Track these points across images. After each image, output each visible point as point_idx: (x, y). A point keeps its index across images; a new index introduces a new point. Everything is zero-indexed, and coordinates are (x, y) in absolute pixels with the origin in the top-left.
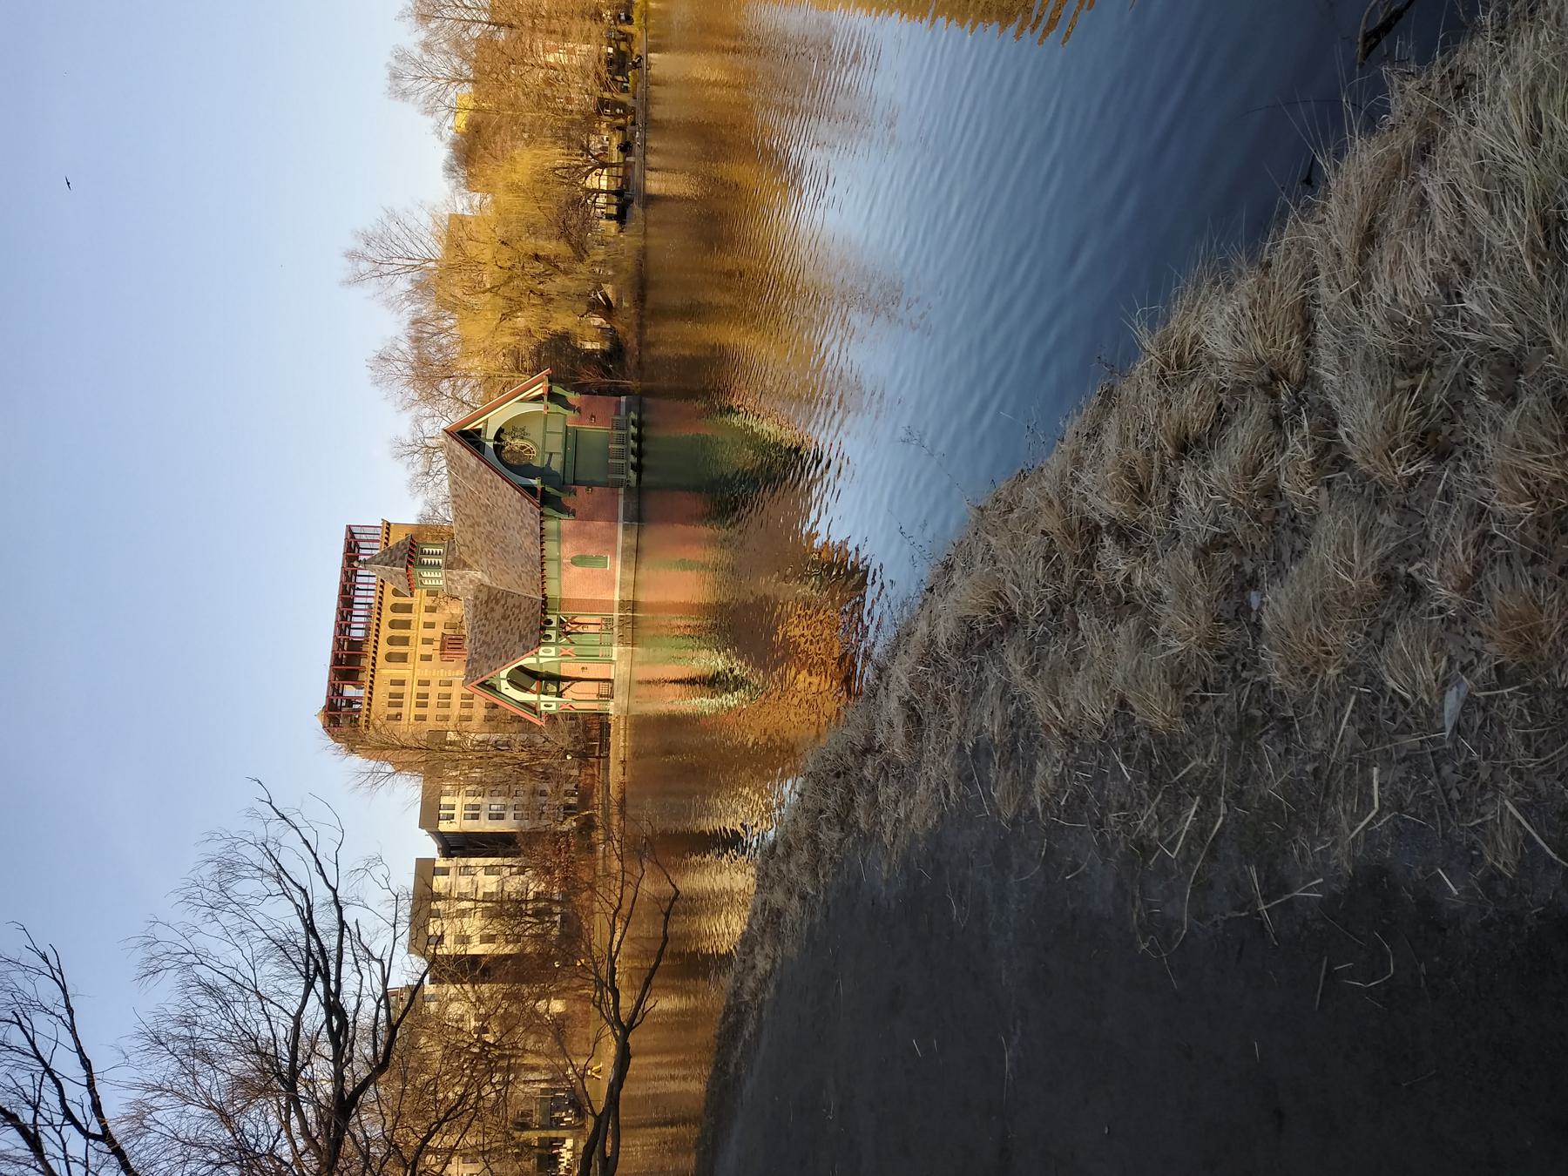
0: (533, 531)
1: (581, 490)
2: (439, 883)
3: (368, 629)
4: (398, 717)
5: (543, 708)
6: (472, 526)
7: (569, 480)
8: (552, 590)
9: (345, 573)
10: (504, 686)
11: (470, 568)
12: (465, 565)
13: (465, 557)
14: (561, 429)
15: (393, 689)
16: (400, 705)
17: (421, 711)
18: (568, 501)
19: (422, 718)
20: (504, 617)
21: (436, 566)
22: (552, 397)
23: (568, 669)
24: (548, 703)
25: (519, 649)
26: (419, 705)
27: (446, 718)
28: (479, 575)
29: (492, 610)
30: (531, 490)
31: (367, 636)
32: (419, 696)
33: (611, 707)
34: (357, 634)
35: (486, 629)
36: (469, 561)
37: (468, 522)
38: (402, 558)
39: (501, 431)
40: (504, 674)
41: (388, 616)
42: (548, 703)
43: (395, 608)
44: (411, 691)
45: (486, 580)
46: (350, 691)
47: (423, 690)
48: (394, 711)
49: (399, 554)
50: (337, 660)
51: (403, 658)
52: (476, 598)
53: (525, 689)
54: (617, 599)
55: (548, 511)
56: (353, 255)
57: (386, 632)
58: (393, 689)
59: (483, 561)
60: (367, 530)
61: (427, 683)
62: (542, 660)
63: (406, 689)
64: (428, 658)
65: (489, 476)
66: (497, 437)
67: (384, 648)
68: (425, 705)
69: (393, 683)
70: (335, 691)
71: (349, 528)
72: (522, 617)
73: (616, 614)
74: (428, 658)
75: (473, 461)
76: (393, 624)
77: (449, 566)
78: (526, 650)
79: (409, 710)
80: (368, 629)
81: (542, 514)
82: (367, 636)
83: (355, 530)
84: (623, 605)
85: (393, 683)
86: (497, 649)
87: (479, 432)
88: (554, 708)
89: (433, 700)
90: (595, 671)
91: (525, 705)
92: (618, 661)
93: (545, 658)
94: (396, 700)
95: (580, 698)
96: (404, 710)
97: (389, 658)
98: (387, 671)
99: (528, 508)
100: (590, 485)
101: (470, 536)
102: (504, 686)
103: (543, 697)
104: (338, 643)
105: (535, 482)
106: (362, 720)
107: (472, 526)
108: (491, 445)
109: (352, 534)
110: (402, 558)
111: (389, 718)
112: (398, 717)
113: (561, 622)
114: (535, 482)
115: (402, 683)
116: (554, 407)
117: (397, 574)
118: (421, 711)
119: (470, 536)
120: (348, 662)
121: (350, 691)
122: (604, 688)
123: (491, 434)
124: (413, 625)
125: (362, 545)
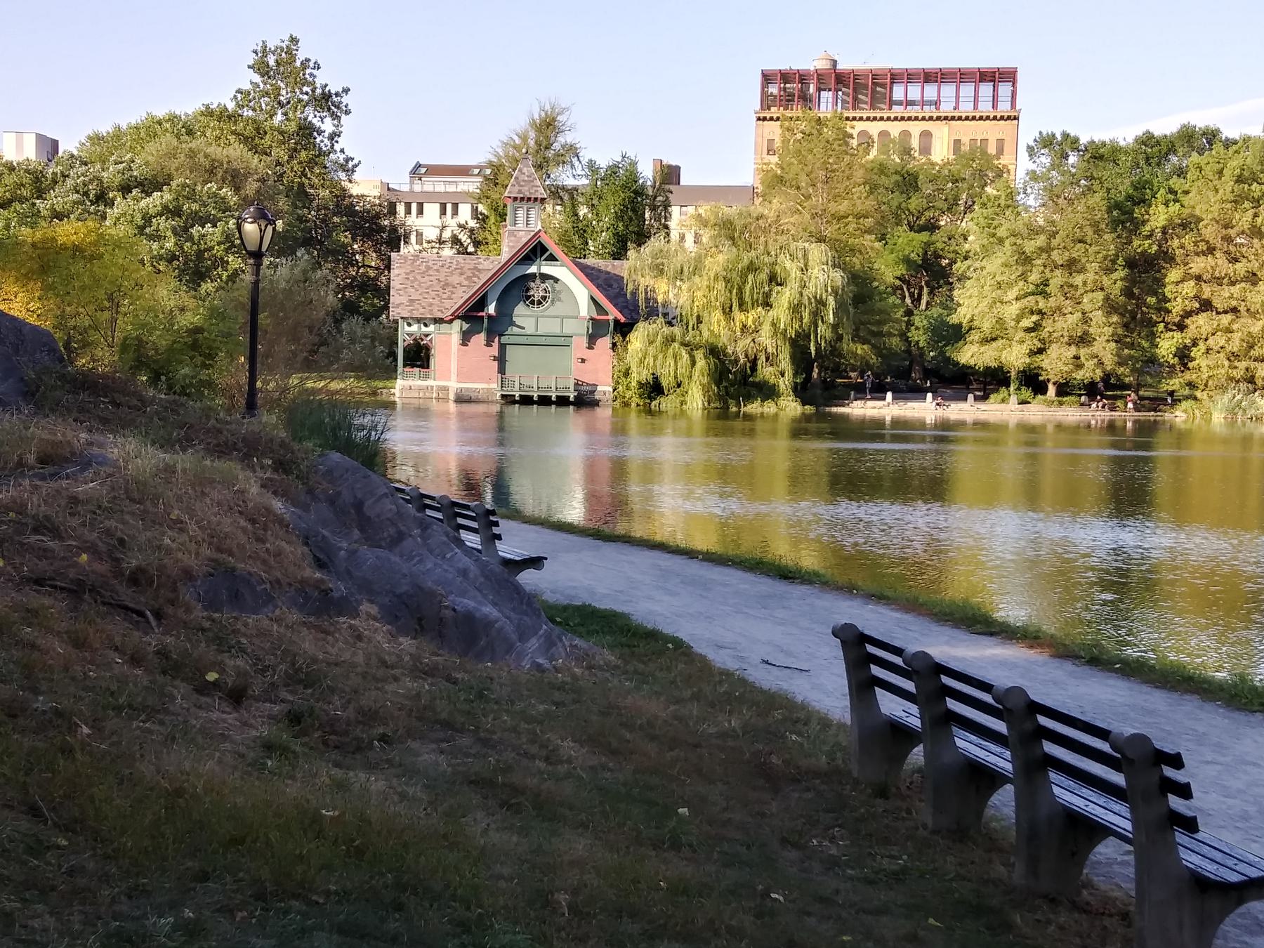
1: (494, 350)
7: (504, 340)
14: (567, 331)
31: (900, 103)
66: (545, 277)
82: (900, 103)
105: (491, 309)
108: (533, 269)
110: (520, 192)
114: (491, 309)
123: (547, 269)
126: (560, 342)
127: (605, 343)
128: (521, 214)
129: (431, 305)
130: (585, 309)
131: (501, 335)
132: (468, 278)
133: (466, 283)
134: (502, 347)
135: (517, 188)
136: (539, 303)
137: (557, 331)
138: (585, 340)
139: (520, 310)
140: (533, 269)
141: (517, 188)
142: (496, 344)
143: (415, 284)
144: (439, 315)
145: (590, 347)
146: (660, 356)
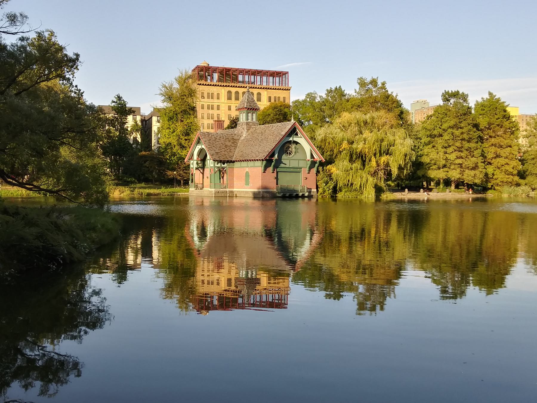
0: (257, 156)
2: (130, 118)
3: (243, 82)
4: (203, 97)
5: (191, 162)
6: (262, 133)
7: (278, 170)
8: (237, 164)
9: (267, 72)
10: (199, 147)
11: (247, 132)
12: (248, 130)
13: (251, 130)
14: (300, 166)
15: (215, 94)
16: (208, 98)
17: (206, 107)
18: (271, 168)
19: (203, 108)
20: (226, 146)
22: (313, 163)
23: (207, 171)
24: (193, 164)
25: (213, 152)
26: (208, 106)
27: (203, 118)
28: (244, 135)
29: (230, 141)
30: (273, 155)
32: (213, 106)
33: (192, 189)
34: (240, 78)
35: (222, 139)
36: (249, 131)
37: (263, 131)
38: (250, 106)
39: (296, 143)
40: (203, 147)
42: (193, 164)
44: (215, 102)
45: (242, 138)
46: (216, 76)
47: (215, 107)
48: (206, 95)
49: (252, 104)
50: (228, 70)
51: (229, 98)
52: (235, 135)
53: (199, 155)
54: (234, 190)
55: (265, 162)
56: (374, 82)
58: (215, 94)
59: (249, 137)
60: (287, 80)
61: (218, 108)
62: (208, 161)
63: (216, 100)
64: (230, 108)
65: (278, 139)
67: (233, 90)
68: (208, 108)
69: (218, 94)
70: (215, 70)
71: (288, 73)
72: (226, 153)
73: (228, 190)
74: (230, 108)
75: (283, 133)
77: (247, 124)
78: (212, 155)
79: (206, 102)
80: (243, 82)
81: (263, 160)
82: (240, 82)
83: (287, 75)
84: (232, 192)
85: (218, 94)
87: (297, 134)
88: (191, 166)
89: (211, 112)
90: (207, 182)
92: (209, 190)
93: (210, 163)
94: (211, 96)
95: (197, 175)
96: (206, 100)
97: (229, 92)
98: (223, 91)
99: (264, 155)
100: (277, 178)
101: (258, 131)
102: (199, 147)
103: (195, 162)
104: (237, 70)
105: (276, 156)
106: (203, 82)
107: (262, 133)
108: (291, 139)
110: (250, 106)
111: (203, 93)
112: (203, 97)
114: (276, 156)
115: (218, 98)
116: (309, 163)
117: (244, 104)
118: (206, 107)
119: (258, 131)
120: (228, 75)
121: (216, 76)
122: (200, 186)
123: (296, 139)
126: (297, 170)
127: (314, 170)
128: (250, 115)
129: (225, 155)
130: (309, 157)
131: (277, 168)
132: (233, 143)
133: (233, 145)
134: (277, 172)
135: (249, 104)
136: (290, 154)
137: (297, 166)
138: (307, 169)
139: (284, 156)
140: (291, 139)
141: (249, 104)
142: (275, 172)
144: (230, 159)
145: (309, 173)
146: (354, 176)
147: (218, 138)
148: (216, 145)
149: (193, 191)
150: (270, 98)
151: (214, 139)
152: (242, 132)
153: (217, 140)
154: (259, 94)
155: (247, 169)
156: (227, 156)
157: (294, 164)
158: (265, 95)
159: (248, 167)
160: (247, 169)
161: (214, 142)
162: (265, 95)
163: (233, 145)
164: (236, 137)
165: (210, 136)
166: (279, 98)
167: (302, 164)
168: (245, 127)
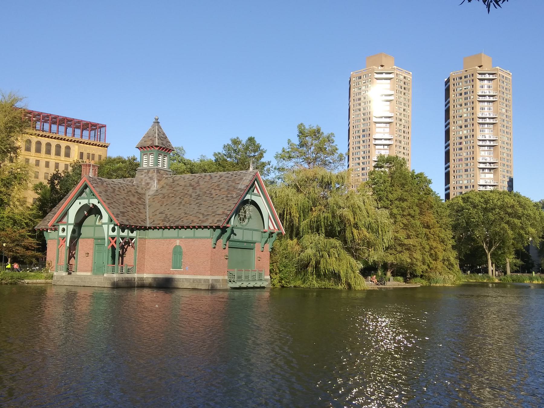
9: (79, 122)
11: (158, 183)
12: (159, 180)
14: (254, 239)
20: (131, 203)
21: (157, 163)
29: (134, 196)
35: (122, 190)
37: (193, 183)
38: (162, 144)
40: (94, 201)
41: (54, 143)
43: (58, 147)
49: (164, 142)
57: (44, 141)
59: (165, 191)
71: (104, 126)
72: (135, 214)
76: (49, 145)
83: (103, 130)
86: (112, 197)
91: (66, 213)
101: (182, 183)
109: (100, 128)
113: (132, 239)
117: (153, 141)
123: (254, 198)
124: (48, 156)
125: (93, 133)
129: (135, 217)
133: (140, 202)
143: (115, 200)
144: (142, 224)
147: (117, 189)
148: (117, 200)
149: (62, 277)
150: (82, 155)
151: (112, 190)
152: (148, 184)
153: (117, 192)
154: (68, 148)
155: (178, 242)
156: (137, 218)
157: (248, 236)
158: (75, 150)
159: (178, 238)
160: (178, 242)
161: (113, 195)
162: (75, 150)
163: (140, 202)
164: (140, 190)
165: (105, 184)
166: (93, 155)
167: (256, 237)
168: (155, 175)
